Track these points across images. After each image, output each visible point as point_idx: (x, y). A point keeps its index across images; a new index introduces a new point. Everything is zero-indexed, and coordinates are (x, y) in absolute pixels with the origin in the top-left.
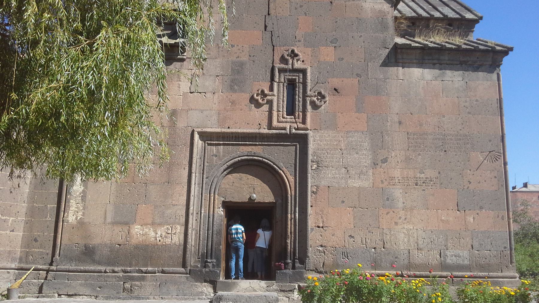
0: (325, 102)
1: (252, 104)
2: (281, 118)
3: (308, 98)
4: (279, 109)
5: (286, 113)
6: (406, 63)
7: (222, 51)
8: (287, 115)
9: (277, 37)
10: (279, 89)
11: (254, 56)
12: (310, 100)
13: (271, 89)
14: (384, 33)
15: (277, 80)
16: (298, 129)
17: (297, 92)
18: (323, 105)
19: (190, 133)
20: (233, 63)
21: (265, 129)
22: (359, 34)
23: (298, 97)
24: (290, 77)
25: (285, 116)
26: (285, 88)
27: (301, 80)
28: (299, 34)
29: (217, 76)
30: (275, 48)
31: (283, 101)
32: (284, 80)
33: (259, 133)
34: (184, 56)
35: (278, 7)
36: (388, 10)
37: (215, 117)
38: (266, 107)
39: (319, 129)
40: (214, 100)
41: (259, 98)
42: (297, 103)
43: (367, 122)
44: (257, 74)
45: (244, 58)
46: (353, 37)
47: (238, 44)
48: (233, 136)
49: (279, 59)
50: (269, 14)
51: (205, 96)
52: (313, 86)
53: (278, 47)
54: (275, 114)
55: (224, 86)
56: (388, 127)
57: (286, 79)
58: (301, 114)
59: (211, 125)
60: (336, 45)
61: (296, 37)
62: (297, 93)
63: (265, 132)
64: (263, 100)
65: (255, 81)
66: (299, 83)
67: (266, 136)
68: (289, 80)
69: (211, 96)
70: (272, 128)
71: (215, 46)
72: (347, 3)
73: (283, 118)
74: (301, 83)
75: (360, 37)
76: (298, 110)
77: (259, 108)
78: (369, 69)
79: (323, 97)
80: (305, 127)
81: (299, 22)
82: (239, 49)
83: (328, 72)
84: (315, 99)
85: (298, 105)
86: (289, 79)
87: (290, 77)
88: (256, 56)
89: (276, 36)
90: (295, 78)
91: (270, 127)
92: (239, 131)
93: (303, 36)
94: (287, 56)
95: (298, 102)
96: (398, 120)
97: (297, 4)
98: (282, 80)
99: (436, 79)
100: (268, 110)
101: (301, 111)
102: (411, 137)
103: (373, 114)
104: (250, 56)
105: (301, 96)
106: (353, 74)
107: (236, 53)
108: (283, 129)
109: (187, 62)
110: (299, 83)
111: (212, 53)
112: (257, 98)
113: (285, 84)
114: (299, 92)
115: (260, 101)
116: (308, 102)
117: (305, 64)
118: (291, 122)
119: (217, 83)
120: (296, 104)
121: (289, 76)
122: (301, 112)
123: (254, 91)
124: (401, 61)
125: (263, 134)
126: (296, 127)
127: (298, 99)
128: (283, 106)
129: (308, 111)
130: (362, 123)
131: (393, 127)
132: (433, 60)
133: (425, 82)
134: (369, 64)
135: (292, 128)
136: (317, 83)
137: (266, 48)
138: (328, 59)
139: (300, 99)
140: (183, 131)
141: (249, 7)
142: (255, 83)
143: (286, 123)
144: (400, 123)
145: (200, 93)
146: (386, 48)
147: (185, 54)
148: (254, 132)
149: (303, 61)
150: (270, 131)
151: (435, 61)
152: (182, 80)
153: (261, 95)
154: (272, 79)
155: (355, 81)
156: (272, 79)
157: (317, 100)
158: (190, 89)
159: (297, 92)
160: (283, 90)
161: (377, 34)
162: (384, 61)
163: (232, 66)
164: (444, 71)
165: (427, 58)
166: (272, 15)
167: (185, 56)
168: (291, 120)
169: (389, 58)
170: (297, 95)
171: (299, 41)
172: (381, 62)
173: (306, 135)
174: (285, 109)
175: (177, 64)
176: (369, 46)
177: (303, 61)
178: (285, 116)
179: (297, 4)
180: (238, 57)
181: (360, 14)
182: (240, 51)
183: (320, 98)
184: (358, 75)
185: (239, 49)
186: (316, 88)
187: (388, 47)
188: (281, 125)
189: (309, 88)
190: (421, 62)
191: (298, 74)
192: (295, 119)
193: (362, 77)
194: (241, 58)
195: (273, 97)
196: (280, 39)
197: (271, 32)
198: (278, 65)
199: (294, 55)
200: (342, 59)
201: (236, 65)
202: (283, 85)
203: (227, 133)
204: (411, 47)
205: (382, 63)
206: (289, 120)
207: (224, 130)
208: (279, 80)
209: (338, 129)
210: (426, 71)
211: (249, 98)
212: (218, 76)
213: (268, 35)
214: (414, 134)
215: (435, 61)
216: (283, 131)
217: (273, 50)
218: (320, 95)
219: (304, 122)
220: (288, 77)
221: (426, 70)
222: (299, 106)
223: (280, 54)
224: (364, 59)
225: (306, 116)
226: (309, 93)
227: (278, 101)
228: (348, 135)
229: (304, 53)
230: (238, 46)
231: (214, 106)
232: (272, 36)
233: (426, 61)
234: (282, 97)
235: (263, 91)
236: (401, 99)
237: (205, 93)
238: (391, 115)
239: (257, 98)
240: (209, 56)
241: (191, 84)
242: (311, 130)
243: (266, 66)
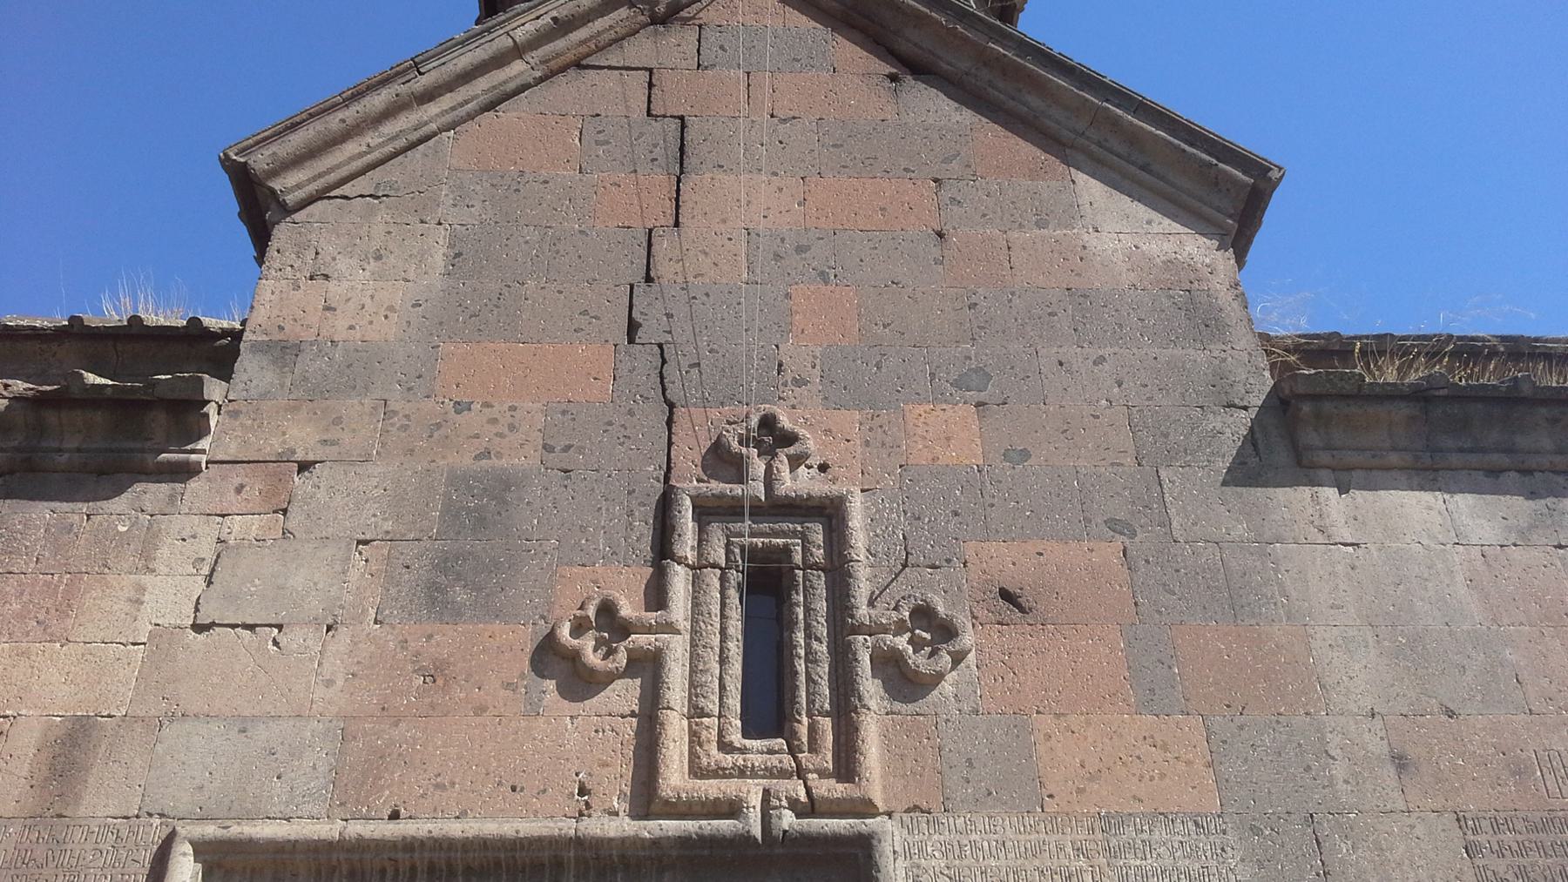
0: (958, 658)
1: (543, 677)
2: (714, 751)
3: (861, 638)
4: (702, 702)
5: (739, 723)
6: (1349, 469)
7: (404, 428)
8: (746, 734)
9: (691, 366)
10: (702, 599)
11: (567, 448)
12: (874, 647)
13: (657, 596)
14: (1212, 347)
15: (691, 557)
16: (811, 808)
17: (800, 611)
18: (949, 677)
19: (146, 857)
20: (457, 480)
21: (617, 814)
22: (1094, 353)
23: (808, 636)
24: (759, 541)
25: (736, 737)
26: (733, 593)
27: (819, 554)
28: (798, 353)
29: (359, 542)
30: (680, 412)
31: (723, 660)
32: (728, 552)
33: (578, 842)
34: (193, 451)
35: (691, 253)
36: (1207, 261)
37: (318, 758)
38: (624, 695)
39: (936, 807)
40: (326, 665)
41: (587, 645)
42: (801, 666)
43: (1210, 765)
44: (583, 529)
45: (520, 458)
46: (1061, 364)
47: (489, 399)
48: (413, 868)
49: (698, 461)
50: (649, 279)
51: (275, 643)
52: (884, 578)
53: (692, 409)
54: (675, 726)
55: (393, 591)
56: (1341, 786)
57: (737, 551)
58: (826, 724)
59: (287, 804)
60: (983, 396)
61: (780, 365)
62: (801, 616)
63: (612, 834)
64: (611, 652)
65: (570, 564)
66: (807, 566)
67: (623, 857)
68: (752, 554)
69: (310, 642)
70: (655, 808)
71: (367, 409)
72: (1014, 235)
73: (725, 747)
74: (816, 567)
75: (1095, 363)
76: (810, 702)
77: (582, 699)
78: (1168, 498)
79: (946, 631)
80: (856, 794)
81: (794, 308)
82: (494, 421)
83: (956, 514)
84: (902, 642)
85: (809, 679)
86: (753, 548)
87: (759, 541)
88: (581, 450)
89: (685, 364)
90: (786, 546)
91: (646, 799)
92: (455, 829)
93: (818, 362)
94: (740, 443)
95: (806, 661)
96: (1386, 750)
97: (783, 240)
98: (719, 555)
99: (1524, 538)
100: (636, 709)
101: (827, 706)
102: (1481, 838)
103: (1239, 720)
104: (548, 448)
105: (822, 631)
106: (1088, 520)
107: (477, 436)
108: (725, 809)
109: (209, 480)
110: (807, 566)
111: (346, 438)
112: (575, 642)
113: (734, 577)
114: (807, 610)
115: (593, 658)
116: (865, 659)
117: (834, 480)
118: (770, 773)
119: (353, 575)
120: (797, 673)
121: (751, 535)
122: (827, 714)
123: (558, 612)
124: (1324, 457)
125: (599, 844)
126: (803, 797)
127: (808, 646)
128: (722, 687)
129: (864, 706)
130: (1181, 766)
131: (1369, 786)
132: (1483, 451)
133: (1476, 552)
134: (1163, 474)
135: (775, 802)
136: (905, 566)
137: (631, 413)
138: (949, 456)
139: (815, 645)
140: (111, 838)
141: (558, 252)
142: (567, 571)
143: (742, 773)
144: (1401, 762)
145: (251, 627)
146: (1231, 405)
147: (204, 444)
148: (545, 832)
149: (823, 468)
150: (643, 823)
151: (1497, 459)
152: (163, 569)
153: (599, 629)
154: (663, 549)
155: (1108, 552)
156: (663, 549)
157: (910, 649)
158: (197, 610)
159: (800, 611)
160: (723, 605)
161: (1178, 352)
162: (1239, 462)
163: (447, 495)
164: (1550, 501)
165: (1449, 443)
166: (664, 281)
167: (203, 451)
168: (774, 760)
169: (1261, 446)
170: (802, 625)
171: (800, 382)
172: (1223, 465)
173: (864, 845)
174: (735, 702)
175: (153, 493)
176: (1149, 399)
177: (823, 468)
178: (736, 737)
179: (783, 240)
180: (486, 454)
181: (1079, 275)
182: (499, 428)
183: (927, 636)
184: (1114, 525)
185: (494, 421)
186: (898, 589)
187: (1241, 404)
188: (712, 788)
189: (862, 589)
190: (1427, 461)
191: (801, 523)
192: (793, 751)
193: (1140, 536)
194: (499, 455)
195: (666, 636)
196: (704, 377)
197: (660, 346)
198: (691, 484)
199: (773, 436)
200: (1025, 455)
201: (470, 488)
202: (723, 579)
203: (379, 845)
204: (1366, 391)
205: (1229, 470)
206: (757, 760)
207: (357, 829)
208: (700, 555)
209: (1051, 805)
210: (1463, 502)
211: (529, 648)
212: (366, 542)
213: (645, 359)
214: (1496, 826)
215: (1497, 459)
216: (725, 826)
217: (670, 422)
218: (925, 623)
219: (846, 766)
220: (747, 541)
221: (1458, 497)
222: (815, 682)
223: (703, 434)
224: (1132, 451)
225: (857, 730)
226: (863, 612)
227: (694, 657)
228: (1114, 842)
229: (828, 432)
230: (487, 405)
231: (320, 692)
232: (664, 362)
233: (1455, 459)
234: (716, 640)
235: (607, 609)
236: (1371, 641)
237: (280, 627)
238: (1342, 719)
239: (575, 642)
240: (331, 452)
241: (210, 583)
242: (890, 815)
243: (629, 493)
